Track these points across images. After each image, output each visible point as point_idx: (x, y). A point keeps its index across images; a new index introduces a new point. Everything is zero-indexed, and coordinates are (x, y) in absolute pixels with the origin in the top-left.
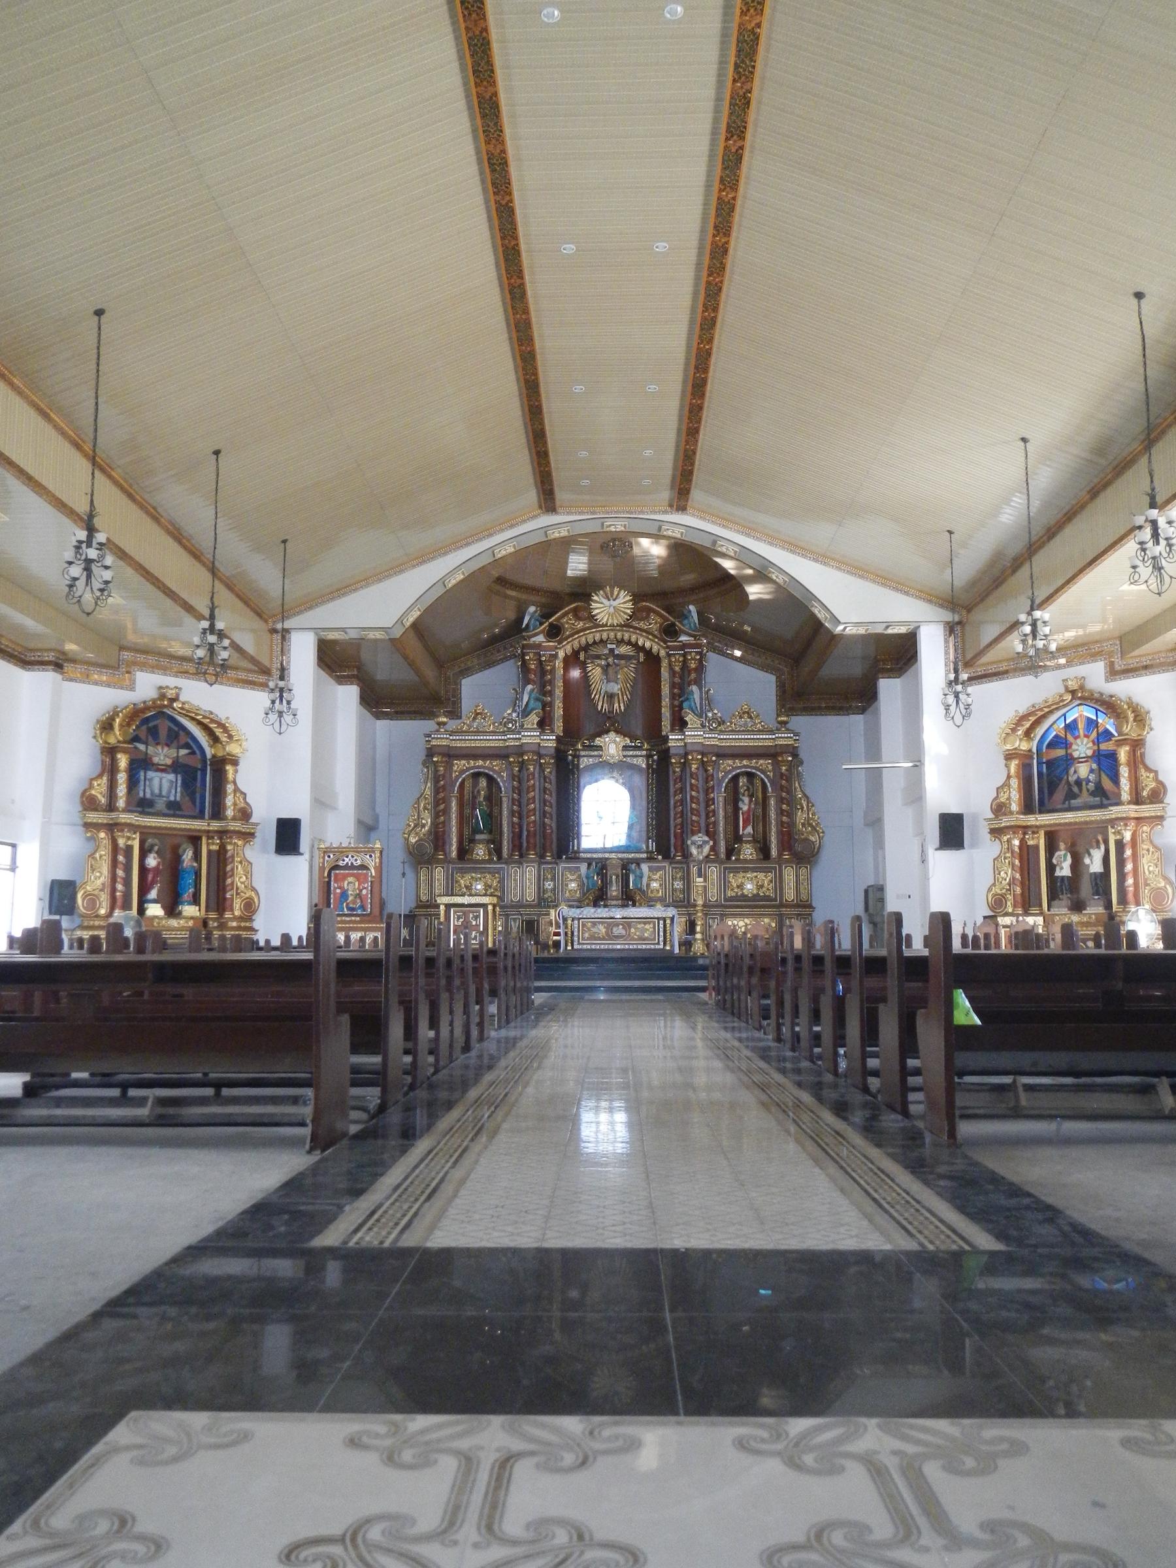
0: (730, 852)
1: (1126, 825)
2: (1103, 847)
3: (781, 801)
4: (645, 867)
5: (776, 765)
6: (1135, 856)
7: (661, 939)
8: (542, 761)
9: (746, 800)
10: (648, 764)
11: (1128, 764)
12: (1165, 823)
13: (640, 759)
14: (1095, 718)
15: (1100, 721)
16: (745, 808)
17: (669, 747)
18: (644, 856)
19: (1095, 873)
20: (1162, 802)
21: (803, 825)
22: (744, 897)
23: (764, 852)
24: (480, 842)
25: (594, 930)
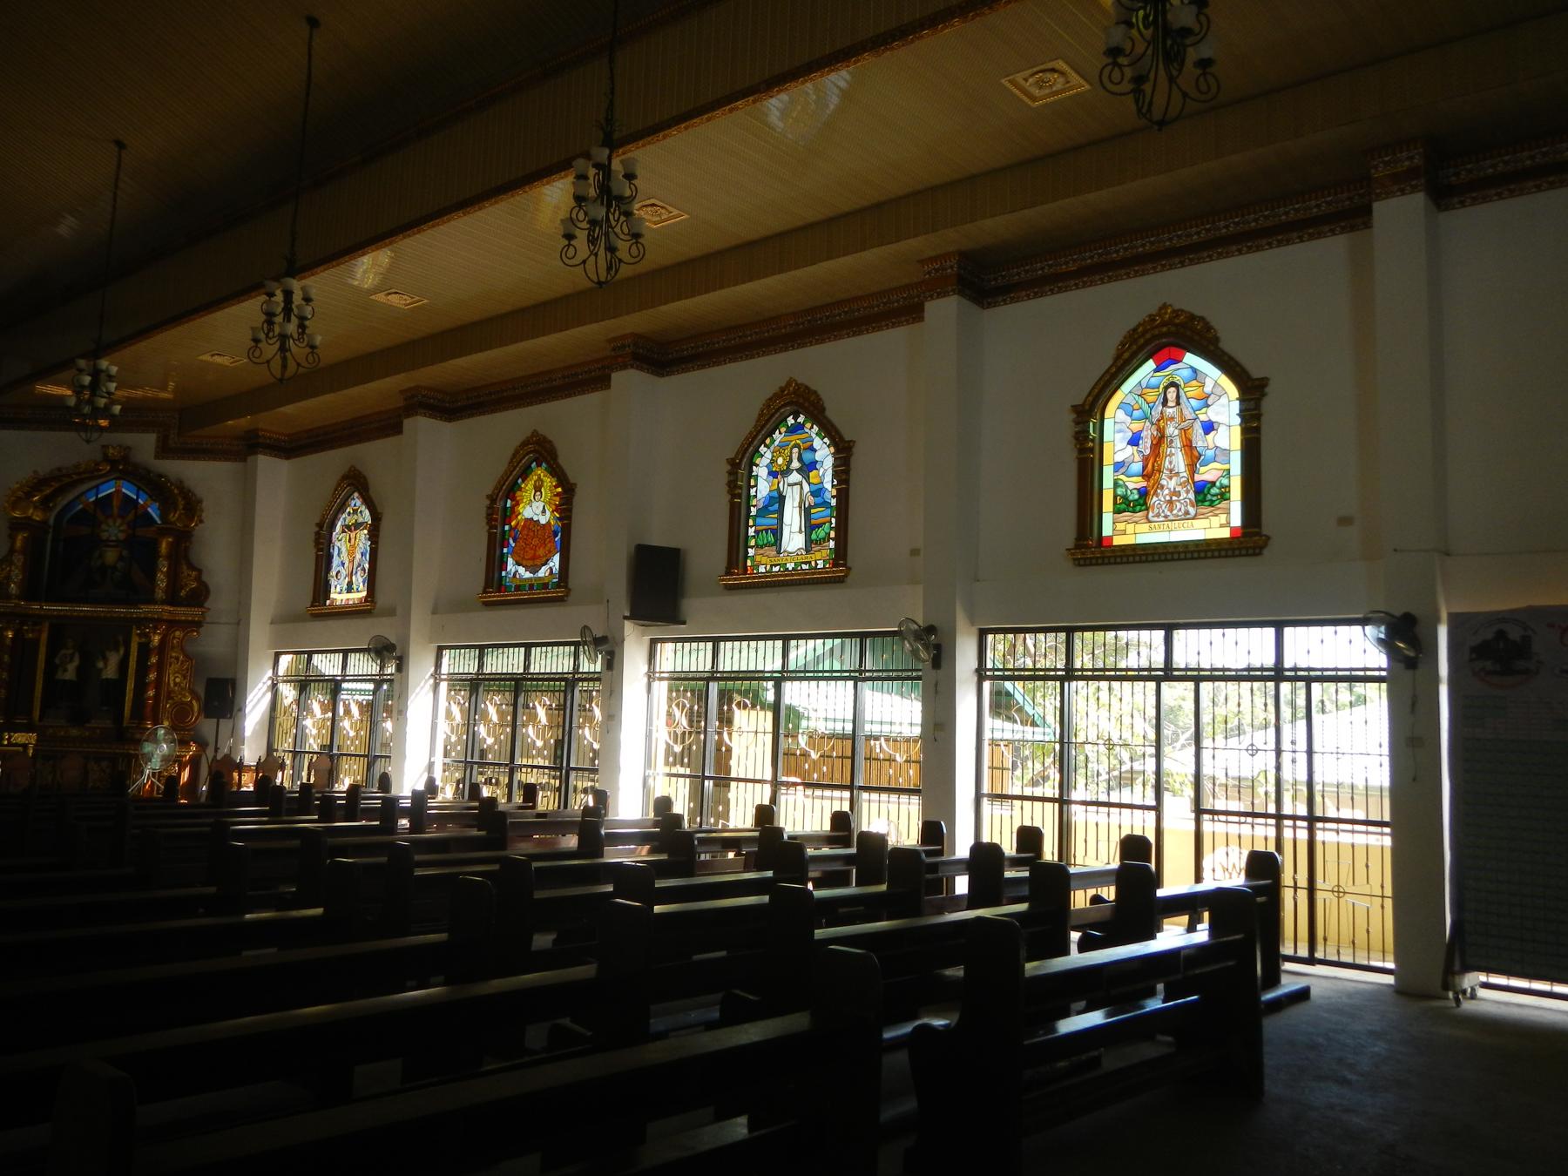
1: (156, 628)
2: (122, 652)
6: (160, 667)
11: (169, 557)
12: (201, 630)
14: (135, 497)
15: (141, 501)
19: (107, 679)
20: (201, 606)
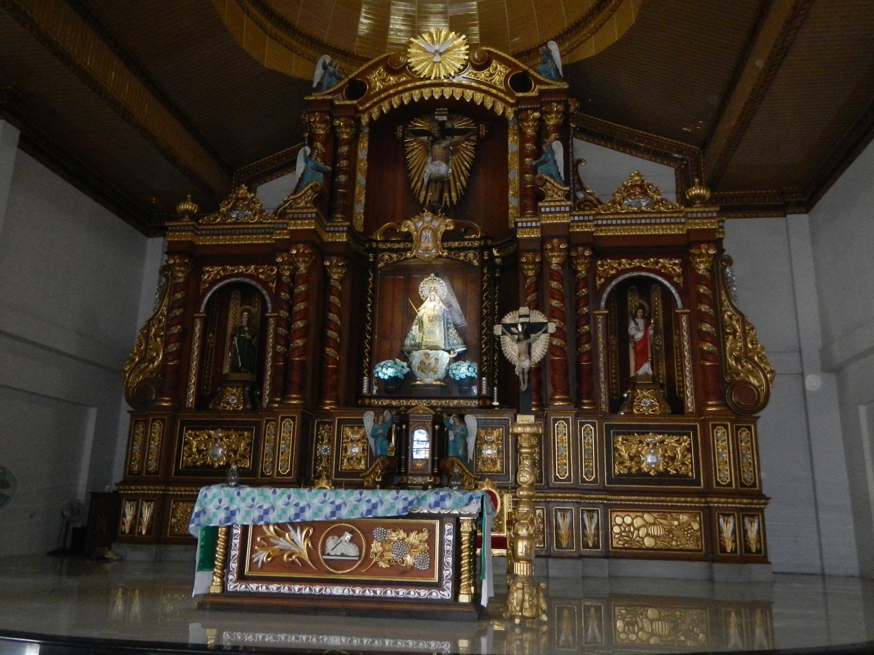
0: (616, 405)
3: (696, 318)
4: (471, 421)
5: (688, 266)
7: (448, 572)
8: (328, 264)
9: (641, 322)
10: (482, 262)
13: (471, 255)
16: (639, 336)
18: (475, 403)
21: (738, 359)
22: (642, 477)
23: (675, 404)
24: (234, 383)
25: (282, 543)
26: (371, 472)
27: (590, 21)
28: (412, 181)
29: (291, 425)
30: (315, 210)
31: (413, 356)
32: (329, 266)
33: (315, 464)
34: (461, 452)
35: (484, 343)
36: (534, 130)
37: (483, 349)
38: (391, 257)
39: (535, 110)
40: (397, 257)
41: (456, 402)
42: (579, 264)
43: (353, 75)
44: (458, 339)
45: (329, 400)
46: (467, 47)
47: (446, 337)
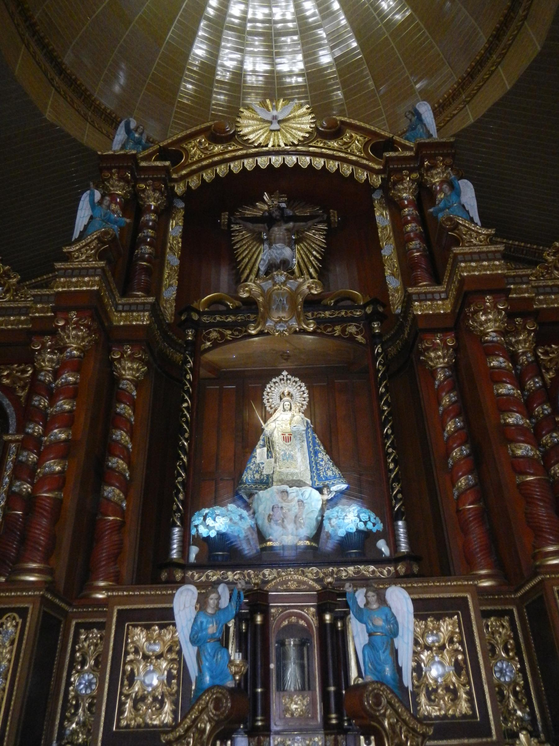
13: (352, 329)
17: (416, 317)
18: (386, 571)
26: (187, 730)
27: (460, 93)
28: (243, 272)
29: (16, 626)
30: (102, 263)
31: (259, 499)
32: (119, 360)
33: (63, 718)
34: (388, 671)
35: (392, 461)
36: (412, 194)
37: (391, 471)
38: (222, 335)
39: (412, 171)
40: (232, 334)
41: (351, 569)
42: (518, 342)
43: (165, 143)
44: (334, 468)
45: (104, 580)
46: (313, 115)
47: (314, 466)
